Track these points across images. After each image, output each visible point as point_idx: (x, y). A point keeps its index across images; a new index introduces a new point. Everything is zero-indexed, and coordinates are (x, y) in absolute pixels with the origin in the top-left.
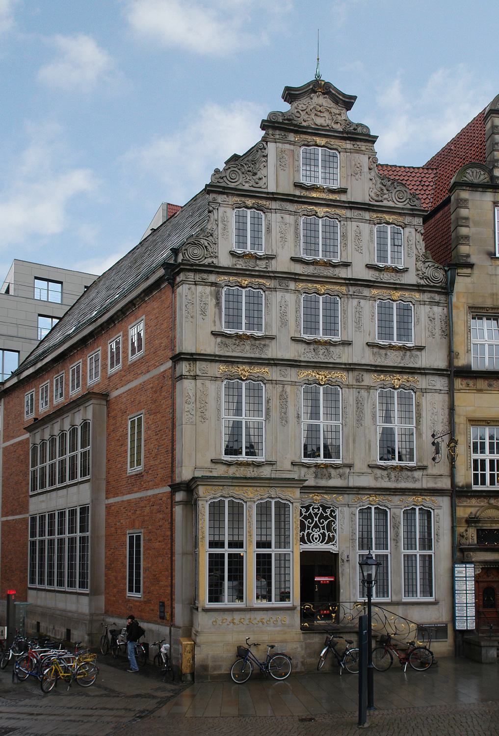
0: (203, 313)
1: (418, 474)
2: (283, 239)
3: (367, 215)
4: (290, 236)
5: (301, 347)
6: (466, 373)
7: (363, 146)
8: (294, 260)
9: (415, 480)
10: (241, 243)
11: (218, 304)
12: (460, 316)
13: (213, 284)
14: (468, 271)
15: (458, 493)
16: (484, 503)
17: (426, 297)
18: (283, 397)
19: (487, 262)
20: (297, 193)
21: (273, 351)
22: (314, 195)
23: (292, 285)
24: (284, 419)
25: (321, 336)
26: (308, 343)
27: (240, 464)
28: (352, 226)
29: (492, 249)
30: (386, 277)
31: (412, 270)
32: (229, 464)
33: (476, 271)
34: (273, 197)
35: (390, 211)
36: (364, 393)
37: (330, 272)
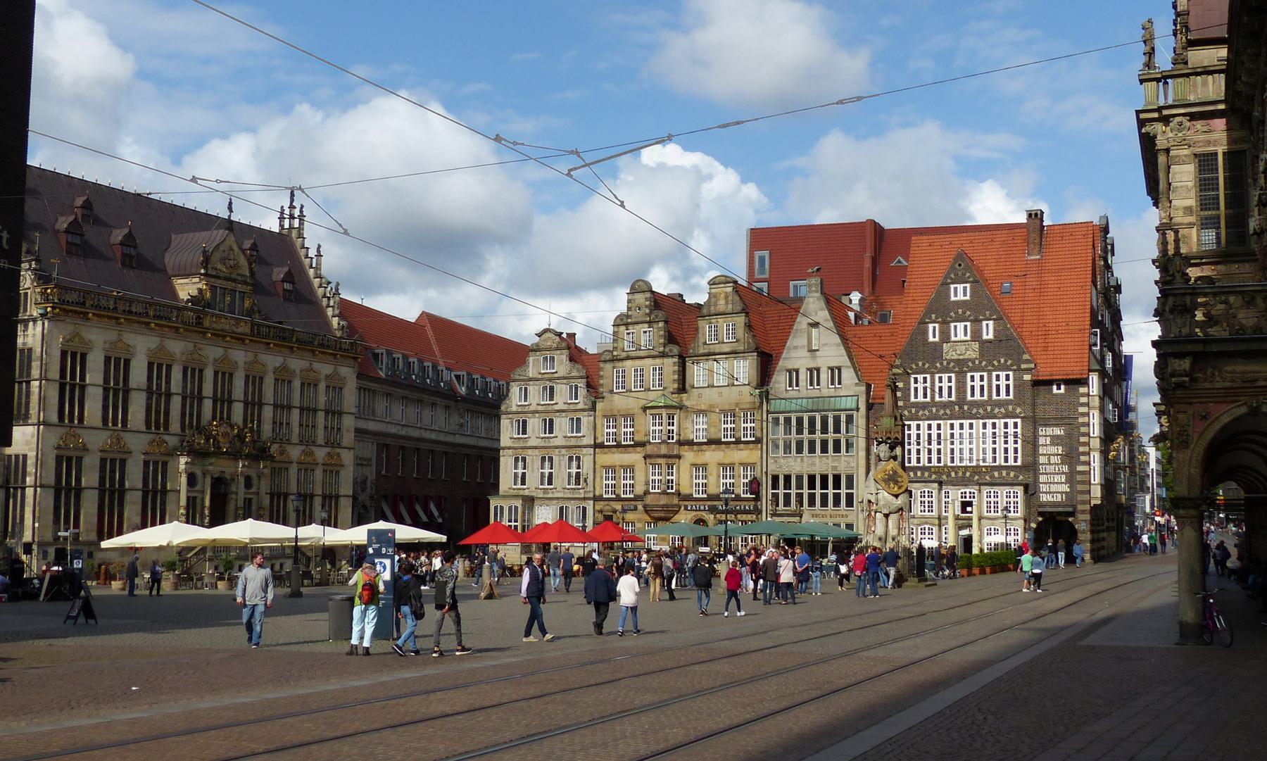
0: (507, 429)
1: (581, 491)
2: (534, 396)
3: (565, 381)
4: (537, 394)
5: (540, 440)
6: (601, 446)
8: (538, 405)
9: (580, 494)
10: (520, 400)
11: (512, 426)
12: (598, 422)
15: (597, 499)
16: (606, 503)
17: (586, 413)
18: (533, 462)
19: (609, 395)
20: (540, 376)
21: (531, 443)
22: (546, 376)
23: (537, 415)
24: (533, 470)
25: (547, 435)
26: (542, 438)
27: (518, 489)
28: (559, 386)
30: (572, 407)
31: (582, 403)
32: (514, 489)
34: (531, 379)
35: (573, 378)
36: (562, 458)
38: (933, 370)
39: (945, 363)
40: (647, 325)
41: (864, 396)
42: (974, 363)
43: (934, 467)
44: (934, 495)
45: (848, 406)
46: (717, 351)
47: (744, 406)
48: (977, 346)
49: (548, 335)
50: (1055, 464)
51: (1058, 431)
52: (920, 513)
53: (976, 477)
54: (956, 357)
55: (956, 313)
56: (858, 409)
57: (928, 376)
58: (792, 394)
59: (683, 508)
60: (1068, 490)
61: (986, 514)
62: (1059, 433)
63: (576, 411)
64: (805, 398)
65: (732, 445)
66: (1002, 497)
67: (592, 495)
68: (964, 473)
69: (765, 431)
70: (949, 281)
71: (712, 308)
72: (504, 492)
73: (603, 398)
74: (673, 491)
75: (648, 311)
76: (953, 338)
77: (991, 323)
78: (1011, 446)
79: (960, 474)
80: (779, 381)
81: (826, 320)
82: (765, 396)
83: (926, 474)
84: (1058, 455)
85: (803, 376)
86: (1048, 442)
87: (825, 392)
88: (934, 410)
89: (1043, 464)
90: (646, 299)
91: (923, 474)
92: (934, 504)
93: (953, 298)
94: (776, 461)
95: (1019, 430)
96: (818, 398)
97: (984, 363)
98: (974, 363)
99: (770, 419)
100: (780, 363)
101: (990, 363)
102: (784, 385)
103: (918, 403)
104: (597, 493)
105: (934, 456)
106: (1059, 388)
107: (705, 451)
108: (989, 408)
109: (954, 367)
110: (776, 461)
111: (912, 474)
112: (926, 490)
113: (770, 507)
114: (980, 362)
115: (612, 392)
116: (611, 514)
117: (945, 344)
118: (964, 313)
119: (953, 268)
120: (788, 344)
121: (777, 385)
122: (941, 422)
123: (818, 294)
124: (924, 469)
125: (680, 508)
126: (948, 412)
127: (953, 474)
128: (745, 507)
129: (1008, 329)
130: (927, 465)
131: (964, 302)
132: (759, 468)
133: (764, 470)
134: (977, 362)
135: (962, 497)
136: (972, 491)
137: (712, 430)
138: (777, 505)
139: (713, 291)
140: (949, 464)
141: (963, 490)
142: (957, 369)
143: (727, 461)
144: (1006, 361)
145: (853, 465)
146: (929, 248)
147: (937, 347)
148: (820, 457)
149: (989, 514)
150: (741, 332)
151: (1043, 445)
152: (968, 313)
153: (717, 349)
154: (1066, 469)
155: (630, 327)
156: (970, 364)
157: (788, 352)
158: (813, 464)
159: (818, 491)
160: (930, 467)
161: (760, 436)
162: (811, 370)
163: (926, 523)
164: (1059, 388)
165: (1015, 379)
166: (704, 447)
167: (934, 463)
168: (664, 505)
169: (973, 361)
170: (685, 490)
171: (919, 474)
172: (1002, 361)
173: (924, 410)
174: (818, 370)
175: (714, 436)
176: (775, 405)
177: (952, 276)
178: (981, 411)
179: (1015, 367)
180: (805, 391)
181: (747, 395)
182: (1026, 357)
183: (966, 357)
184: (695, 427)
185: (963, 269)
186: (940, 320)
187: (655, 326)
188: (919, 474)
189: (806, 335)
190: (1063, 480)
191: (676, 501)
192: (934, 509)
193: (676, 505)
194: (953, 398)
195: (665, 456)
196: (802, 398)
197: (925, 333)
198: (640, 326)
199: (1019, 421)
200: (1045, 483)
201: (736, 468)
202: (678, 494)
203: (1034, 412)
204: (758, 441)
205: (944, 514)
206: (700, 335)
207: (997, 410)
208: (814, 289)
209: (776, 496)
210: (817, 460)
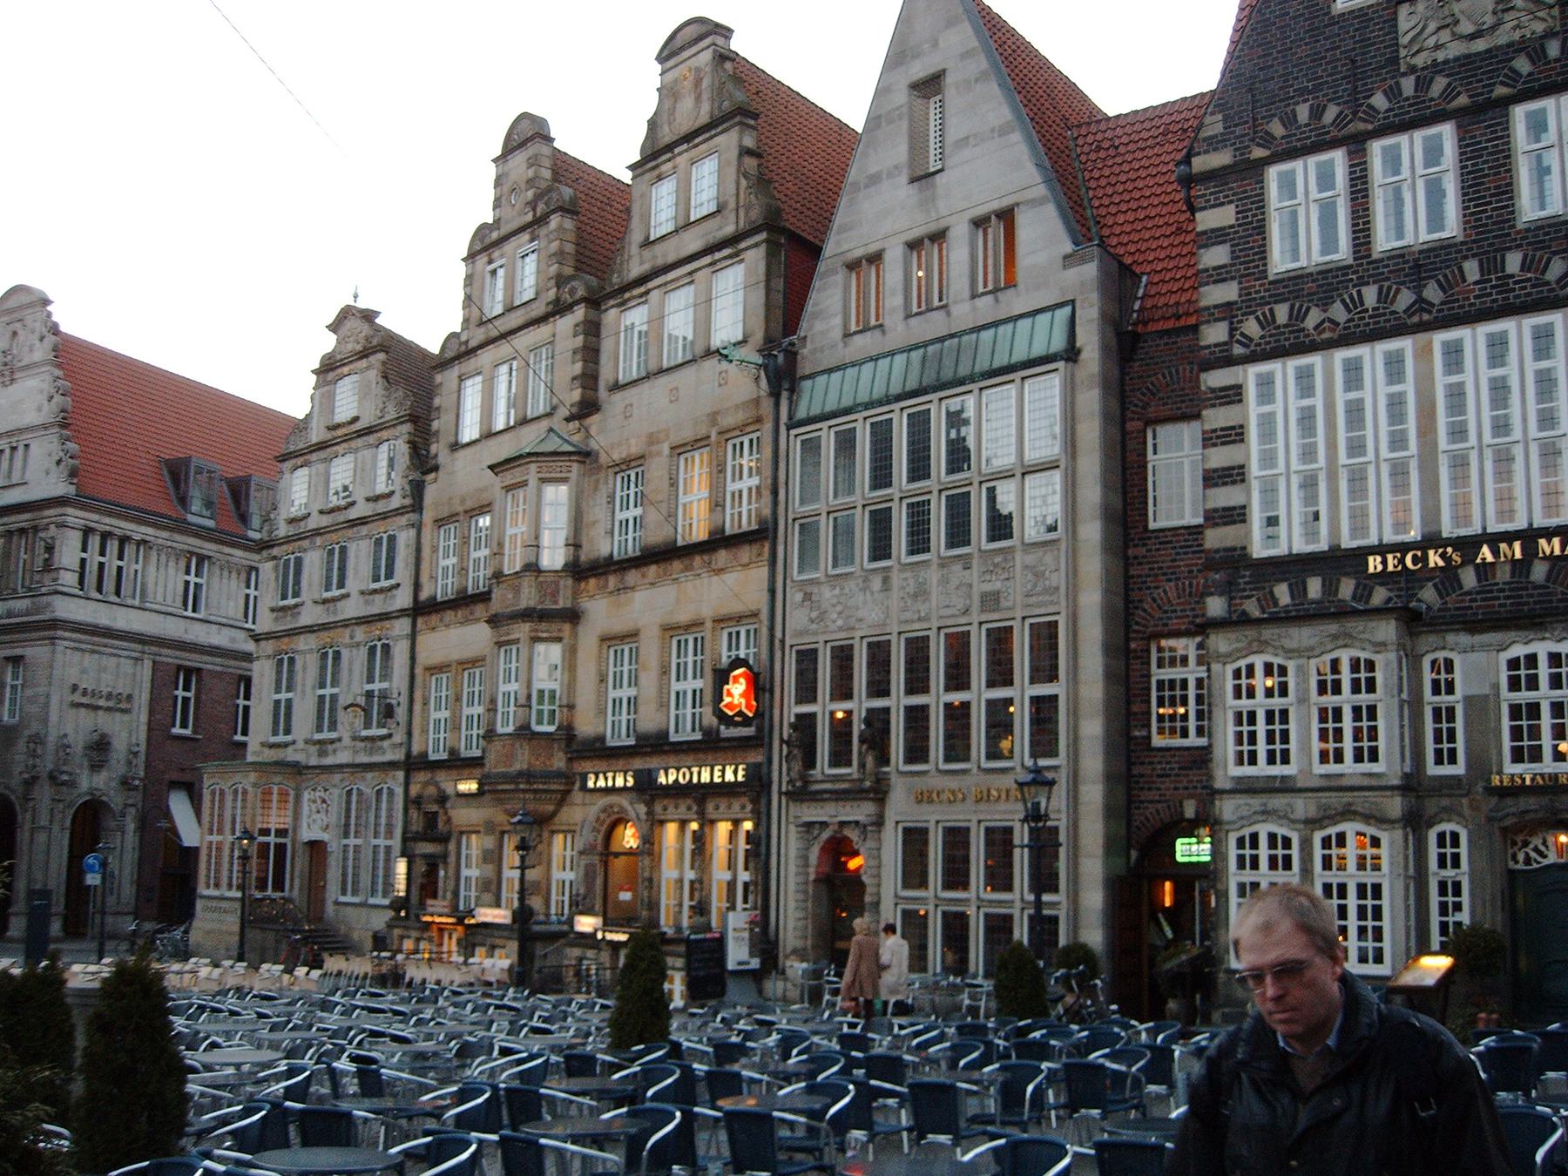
1: (386, 744)
7: (372, 359)
9: (383, 751)
13: (275, 558)
14: (433, 475)
15: (414, 764)
18: (304, 668)
20: (329, 435)
23: (319, 540)
24: (303, 692)
29: (452, 439)
33: (441, 473)
37: (341, 517)
40: (526, 237)
41: (1094, 297)
43: (1382, 550)
44: (1379, 676)
45: (1038, 350)
46: (672, 258)
47: (729, 420)
49: (350, 324)
52: (1320, 769)
54: (1455, 50)
56: (1071, 354)
59: (577, 785)
63: (384, 516)
67: (399, 755)
69: (782, 492)
71: (666, 129)
72: (254, 753)
73: (436, 469)
74: (552, 729)
75: (530, 194)
83: (1347, 588)
87: (964, 313)
90: (533, 162)
91: (1330, 588)
92: (1381, 724)
94: (808, 596)
96: (942, 340)
100: (829, 249)
102: (837, 321)
104: (416, 749)
107: (633, 588)
109: (1449, 94)
111: (1283, 593)
112: (1345, 656)
115: (456, 446)
116: (435, 808)
117: (1404, 10)
120: (854, 174)
121: (819, 326)
122: (1406, 344)
125: (573, 783)
126: (1432, 293)
127: (1469, 578)
130: (1347, 542)
132: (765, 631)
133: (779, 634)
135: (1514, 684)
137: (653, 516)
138: (810, 761)
139: (670, 76)
140: (1447, 530)
141: (1519, 651)
142: (1463, 100)
143: (683, 617)
148: (944, 563)
153: (668, 252)
155: (496, 254)
156: (1523, 65)
158: (921, 593)
161: (767, 512)
162: (914, 245)
163: (1347, 814)
166: (632, 576)
168: (520, 774)
169: (1533, 48)
170: (586, 726)
171: (1314, 587)
173: (1325, 305)
175: (656, 535)
176: (817, 395)
180: (901, 327)
183: (1503, 37)
184: (619, 516)
187: (543, 231)
188: (1314, 587)
189: (904, 125)
191: (559, 762)
192: (1382, 743)
193: (558, 775)
195: (527, 615)
196: (892, 354)
198: (514, 242)
201: (708, 635)
202: (567, 734)
204: (763, 534)
205: (1433, 770)
206: (635, 223)
209: (805, 724)
210: (933, 576)
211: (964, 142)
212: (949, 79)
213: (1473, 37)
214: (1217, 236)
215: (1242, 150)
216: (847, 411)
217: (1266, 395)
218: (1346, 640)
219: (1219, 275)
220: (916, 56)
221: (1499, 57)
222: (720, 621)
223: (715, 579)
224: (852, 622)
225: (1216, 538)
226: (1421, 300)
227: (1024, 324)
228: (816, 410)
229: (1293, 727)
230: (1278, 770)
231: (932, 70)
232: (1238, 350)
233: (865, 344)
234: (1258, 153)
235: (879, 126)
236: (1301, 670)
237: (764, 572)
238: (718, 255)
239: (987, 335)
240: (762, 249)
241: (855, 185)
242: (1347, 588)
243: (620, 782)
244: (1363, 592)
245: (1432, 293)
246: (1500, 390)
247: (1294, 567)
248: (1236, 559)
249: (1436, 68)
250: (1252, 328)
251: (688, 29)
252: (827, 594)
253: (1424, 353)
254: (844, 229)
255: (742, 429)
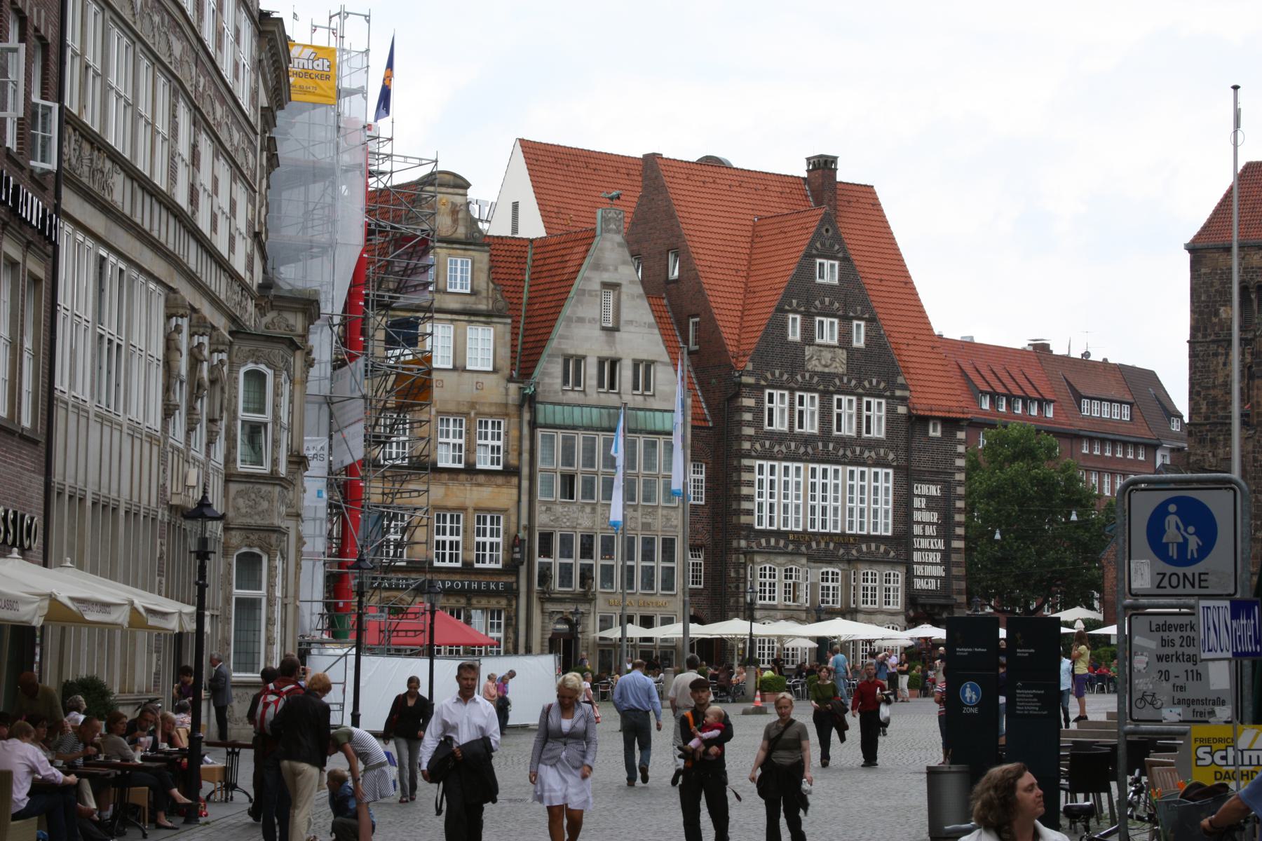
38: (792, 385)
39: (807, 375)
42: (841, 380)
47: (487, 410)
48: (845, 356)
50: (931, 537)
51: (934, 490)
53: (842, 551)
54: (819, 369)
55: (822, 302)
57: (786, 393)
58: (573, 397)
60: (943, 574)
61: (862, 606)
62: (935, 494)
64: (596, 407)
65: (462, 477)
66: (881, 580)
68: (827, 544)
70: (814, 252)
76: (818, 341)
77: (863, 323)
78: (881, 506)
79: (823, 545)
80: (549, 373)
81: (632, 282)
82: (529, 401)
84: (933, 524)
85: (591, 370)
86: (923, 506)
88: (793, 445)
89: (918, 536)
91: (777, 542)
93: (818, 280)
94: (548, 509)
95: (890, 485)
97: (853, 382)
98: (841, 380)
99: (539, 433)
100: (554, 344)
101: (860, 383)
103: (772, 433)
105: (791, 515)
106: (934, 430)
108: (858, 449)
110: (548, 509)
111: (763, 541)
113: (536, 587)
114: (849, 381)
117: (807, 347)
118: (832, 303)
119: (818, 234)
120: (567, 311)
121: (547, 380)
122: (801, 465)
123: (618, 238)
124: (778, 534)
126: (810, 450)
127: (814, 545)
128: (488, 585)
129: (881, 336)
131: (832, 287)
132: (513, 519)
134: (845, 380)
136: (836, 570)
141: (824, 570)
142: (821, 387)
144: (878, 383)
145: (675, 523)
146: (686, 182)
147: (798, 348)
149: (865, 606)
150: (483, 282)
151: (918, 509)
152: (837, 305)
154: (940, 545)
156: (837, 381)
157: (568, 326)
159: (597, 562)
160: (786, 533)
164: (934, 430)
165: (888, 411)
167: (791, 527)
171: (773, 541)
172: (874, 381)
173: (780, 445)
174: (614, 363)
177: (818, 245)
178: (849, 453)
179: (888, 393)
180: (595, 395)
181: (498, 391)
182: (900, 380)
183: (832, 371)
185: (832, 237)
186: (802, 309)
188: (773, 541)
189: (599, 300)
190: (938, 561)
194: (816, 431)
197: (784, 327)
199: (891, 471)
200: (918, 563)
203: (907, 460)
204: (510, 472)
207: (866, 454)
208: (612, 226)
211: (630, 322)
212: (624, 289)
213: (826, 366)
214: (749, 409)
215: (758, 379)
216: (574, 428)
217: (761, 472)
218: (791, 562)
219: (749, 424)
220: (606, 270)
221: (831, 376)
222: (476, 510)
223: (475, 488)
224: (575, 524)
225: (744, 519)
226: (806, 451)
227: (658, 414)
228: (550, 421)
229: (776, 588)
230: (772, 602)
231: (614, 281)
232: (753, 453)
233: (573, 397)
234: (763, 383)
235: (584, 295)
236: (780, 571)
237: (515, 491)
238: (473, 318)
239: (640, 413)
240: (508, 328)
241: (569, 320)
242: (782, 543)
243: (402, 583)
244: (786, 546)
245: (810, 450)
246: (824, 486)
247: (767, 534)
248: (750, 527)
249: (816, 373)
250: (758, 446)
251: (447, 177)
252: (559, 509)
253: (806, 469)
254: (562, 337)
255: (491, 416)
